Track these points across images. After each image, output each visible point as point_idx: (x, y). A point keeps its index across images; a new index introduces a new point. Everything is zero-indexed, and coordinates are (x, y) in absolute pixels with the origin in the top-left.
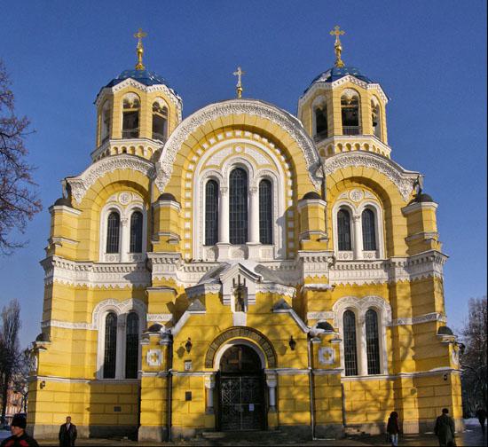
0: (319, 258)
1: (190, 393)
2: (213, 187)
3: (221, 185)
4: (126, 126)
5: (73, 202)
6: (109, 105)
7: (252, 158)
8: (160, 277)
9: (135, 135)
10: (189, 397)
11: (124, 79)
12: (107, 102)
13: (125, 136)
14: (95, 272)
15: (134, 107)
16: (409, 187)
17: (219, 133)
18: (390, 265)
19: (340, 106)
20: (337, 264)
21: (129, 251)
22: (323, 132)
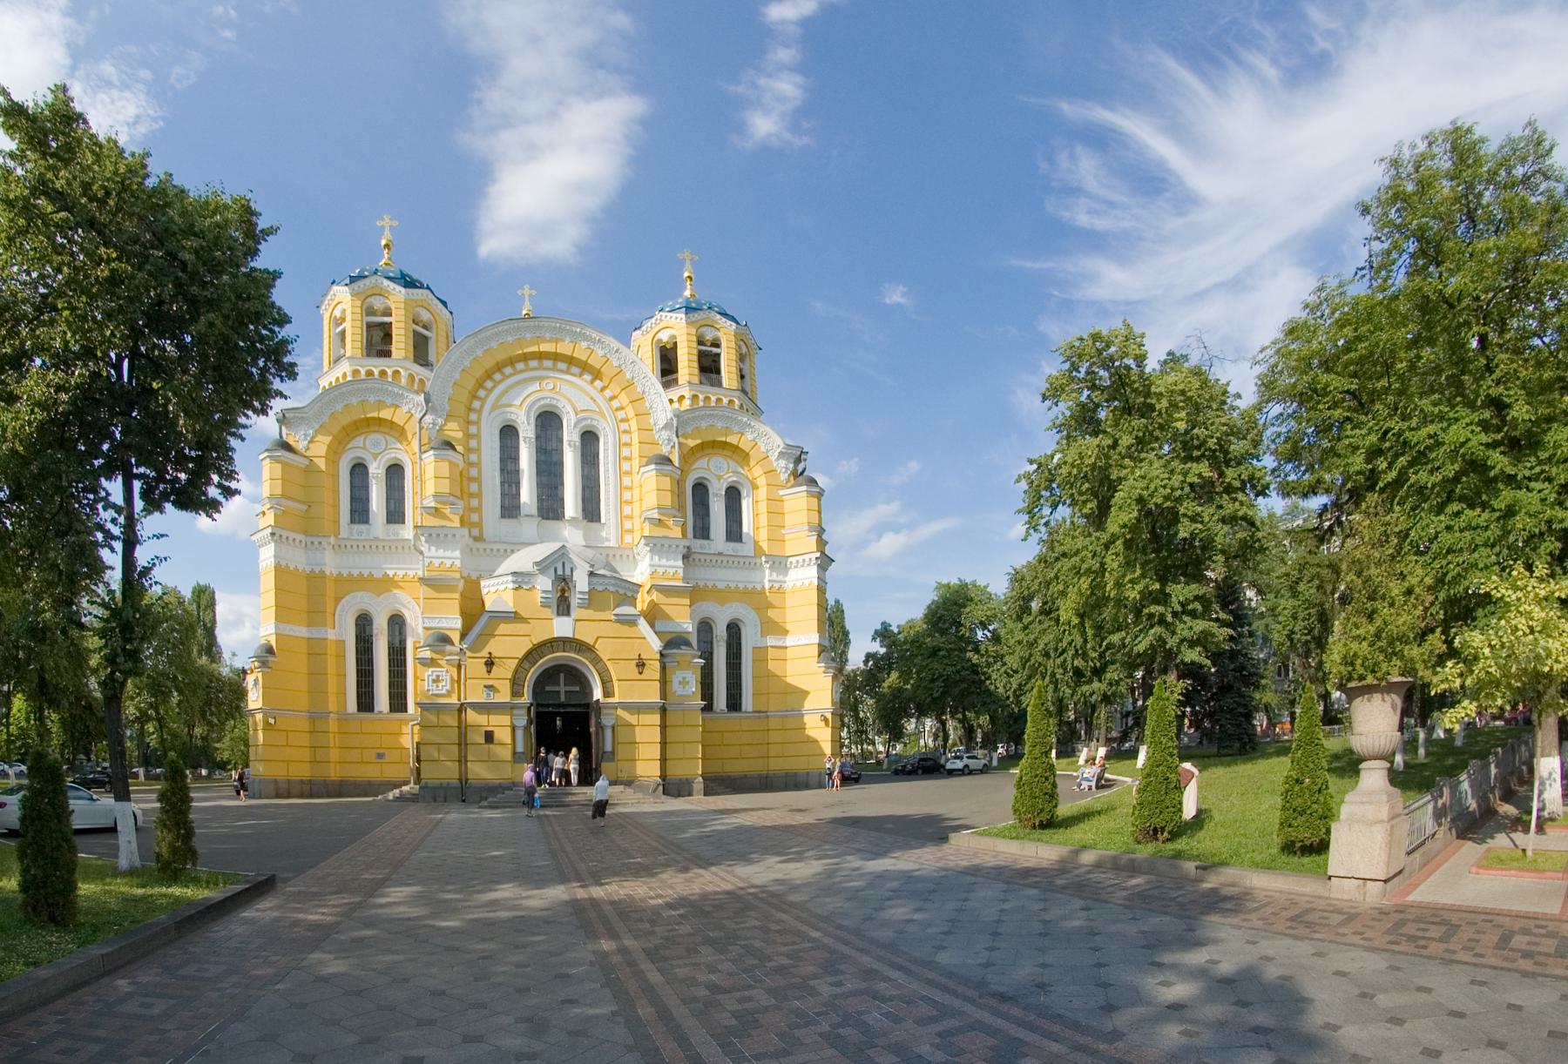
2: (509, 433)
20: (694, 556)
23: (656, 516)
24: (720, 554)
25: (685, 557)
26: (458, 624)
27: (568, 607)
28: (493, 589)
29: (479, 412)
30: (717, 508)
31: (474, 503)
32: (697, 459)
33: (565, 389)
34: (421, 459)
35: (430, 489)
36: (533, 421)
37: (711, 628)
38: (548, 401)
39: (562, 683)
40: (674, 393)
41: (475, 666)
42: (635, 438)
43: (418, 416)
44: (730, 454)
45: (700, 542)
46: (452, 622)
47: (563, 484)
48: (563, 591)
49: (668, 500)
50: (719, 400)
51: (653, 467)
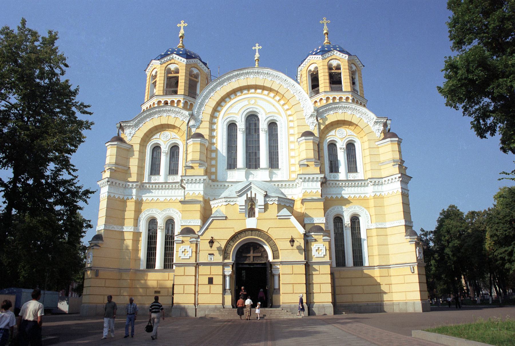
0: (313, 178)
2: (232, 127)
6: (156, 72)
7: (264, 109)
8: (191, 193)
9: (176, 93)
10: (211, 281)
11: (169, 55)
16: (382, 128)
19: (327, 71)
22: (316, 89)
23: (306, 163)
25: (322, 184)
26: (199, 222)
27: (254, 213)
28: (216, 206)
30: (342, 156)
31: (213, 162)
34: (187, 143)
35: (190, 158)
36: (244, 120)
37: (342, 220)
38: (251, 110)
40: (317, 98)
41: (204, 245)
42: (296, 124)
44: (348, 127)
46: (195, 223)
47: (259, 150)
48: (252, 205)
49: (311, 154)
50: (341, 98)
51: (303, 138)
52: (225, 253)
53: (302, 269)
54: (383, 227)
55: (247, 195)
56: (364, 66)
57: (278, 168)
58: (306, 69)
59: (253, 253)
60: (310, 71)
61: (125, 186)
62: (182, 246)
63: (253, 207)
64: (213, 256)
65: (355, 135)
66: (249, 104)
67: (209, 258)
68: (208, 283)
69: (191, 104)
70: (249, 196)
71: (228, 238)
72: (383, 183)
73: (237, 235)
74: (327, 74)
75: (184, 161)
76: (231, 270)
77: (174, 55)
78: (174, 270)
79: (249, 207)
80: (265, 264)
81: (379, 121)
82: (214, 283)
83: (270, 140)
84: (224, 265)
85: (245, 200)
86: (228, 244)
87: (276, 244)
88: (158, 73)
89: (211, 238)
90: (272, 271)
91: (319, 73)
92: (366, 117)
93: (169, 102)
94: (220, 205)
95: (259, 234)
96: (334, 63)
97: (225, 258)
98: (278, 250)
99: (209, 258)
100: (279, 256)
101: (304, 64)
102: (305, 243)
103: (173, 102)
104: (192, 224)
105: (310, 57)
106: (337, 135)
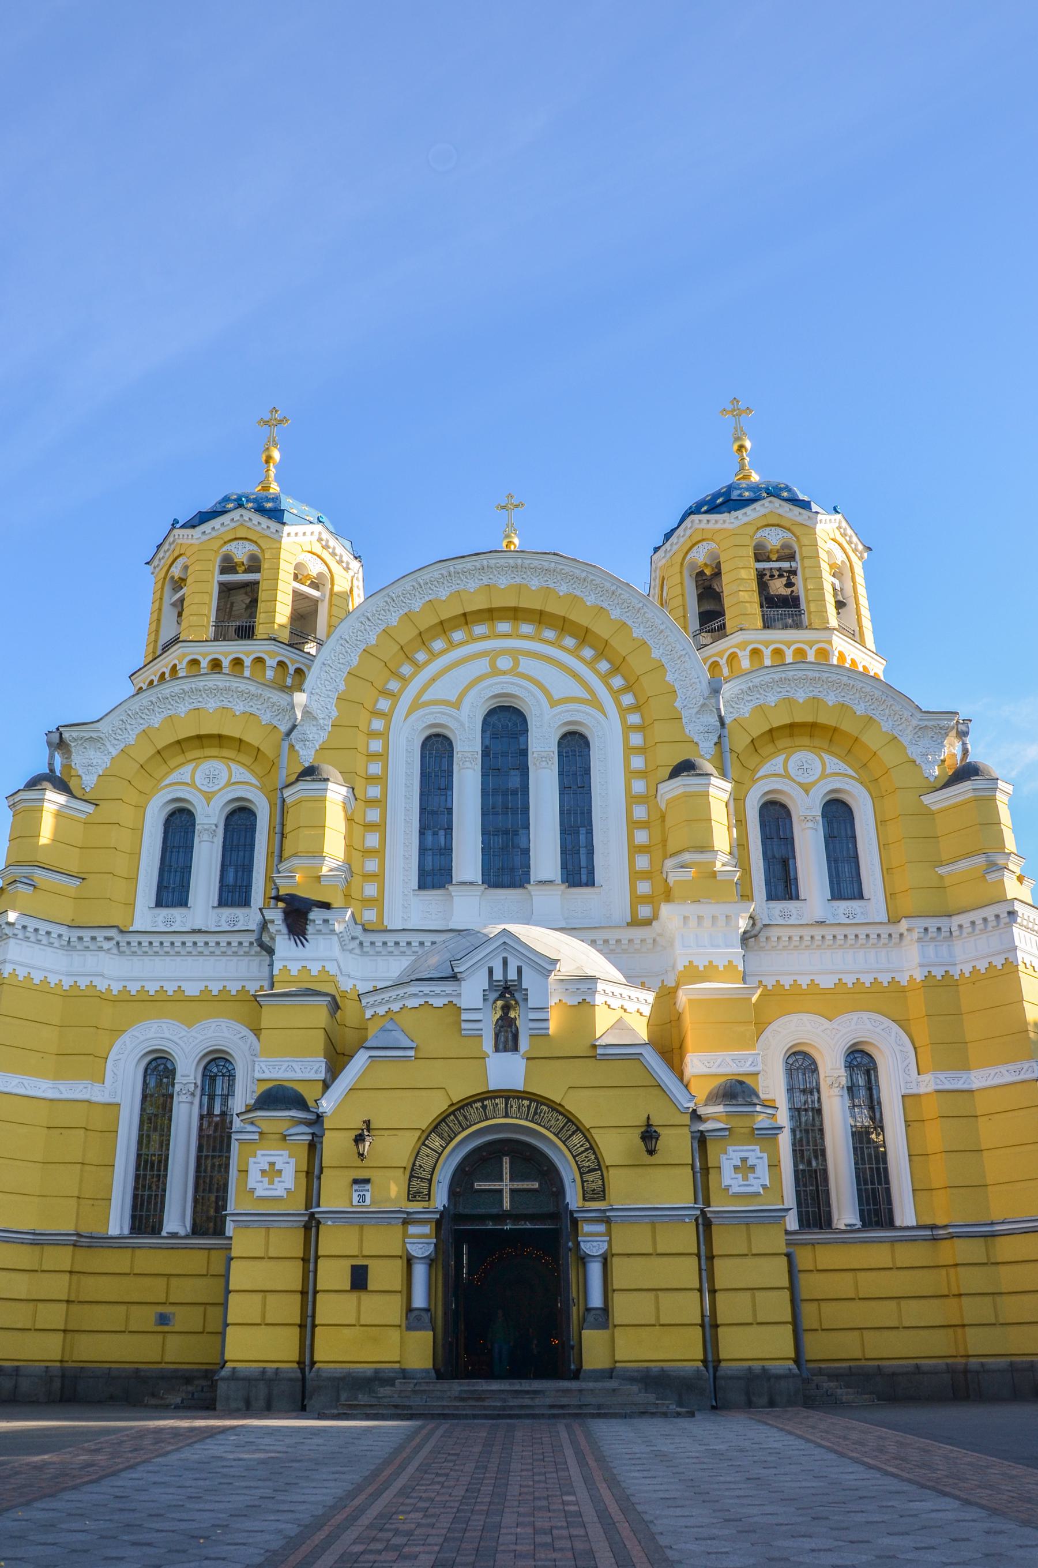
1: (366, 1267)
3: (459, 748)
4: (225, 611)
5: (73, 784)
6: (186, 568)
8: (294, 968)
9: (246, 633)
10: (359, 1279)
12: (181, 561)
13: (220, 635)
14: (121, 953)
15: (249, 570)
17: (455, 628)
18: (901, 935)
21: (215, 900)
22: (715, 624)
24: (821, 923)
27: (516, 1037)
28: (381, 1010)
29: (387, 716)
32: (764, 759)
33: (527, 665)
34: (284, 800)
39: (506, 1175)
43: (284, 728)
45: (778, 906)
48: (506, 1008)
52: (411, 1176)
53: (686, 1238)
54: (959, 1085)
55: (491, 971)
56: (870, 549)
57: (591, 883)
58: (680, 560)
59: (511, 1180)
60: (693, 565)
61: (69, 942)
62: (259, 1153)
63: (512, 1015)
64: (368, 1187)
65: (851, 772)
66: (495, 672)
67: (355, 1195)
68: (349, 1288)
69: (299, 672)
70: (498, 975)
71: (425, 1123)
72: (954, 934)
73: (453, 1113)
74: (753, 574)
75: (276, 859)
76: (434, 1240)
77: (247, 515)
78: (230, 1238)
79: (498, 1016)
80: (555, 1216)
81: (930, 724)
82: (371, 1286)
83: (564, 789)
84: (407, 1222)
85: (484, 990)
86: (424, 1144)
87: (591, 1148)
88: (190, 571)
89: (361, 1125)
90: (578, 1244)
91: (723, 572)
92: (887, 712)
93: (226, 663)
94: (396, 1007)
95: (532, 1110)
96: (774, 539)
97: (413, 1196)
98: (600, 1169)
99: (355, 1195)
100: (604, 1191)
101: (671, 545)
102: (696, 1145)
103: (238, 662)
104: (299, 1075)
105: (692, 522)
106: (792, 772)
